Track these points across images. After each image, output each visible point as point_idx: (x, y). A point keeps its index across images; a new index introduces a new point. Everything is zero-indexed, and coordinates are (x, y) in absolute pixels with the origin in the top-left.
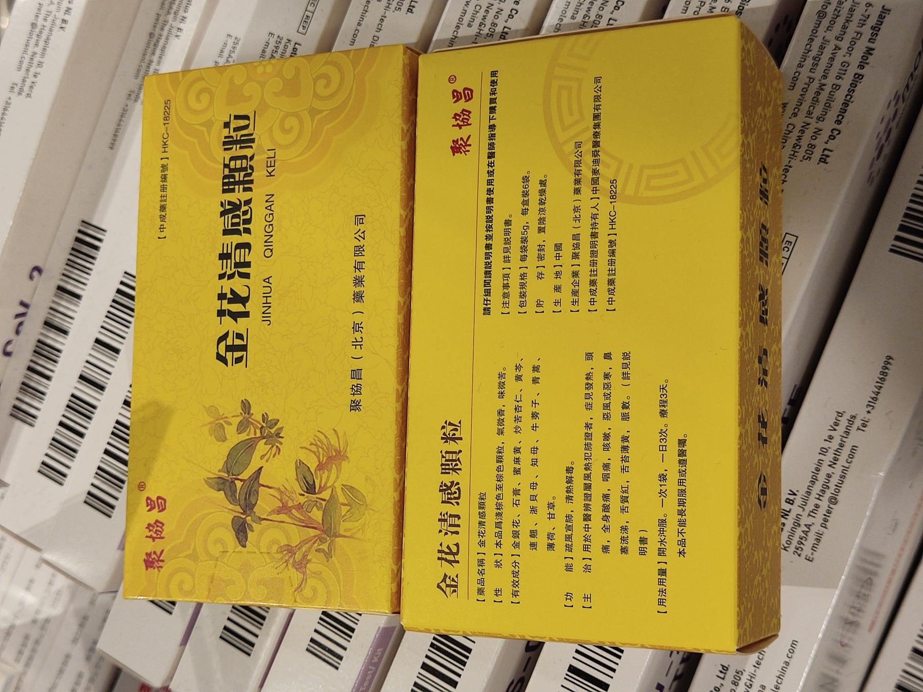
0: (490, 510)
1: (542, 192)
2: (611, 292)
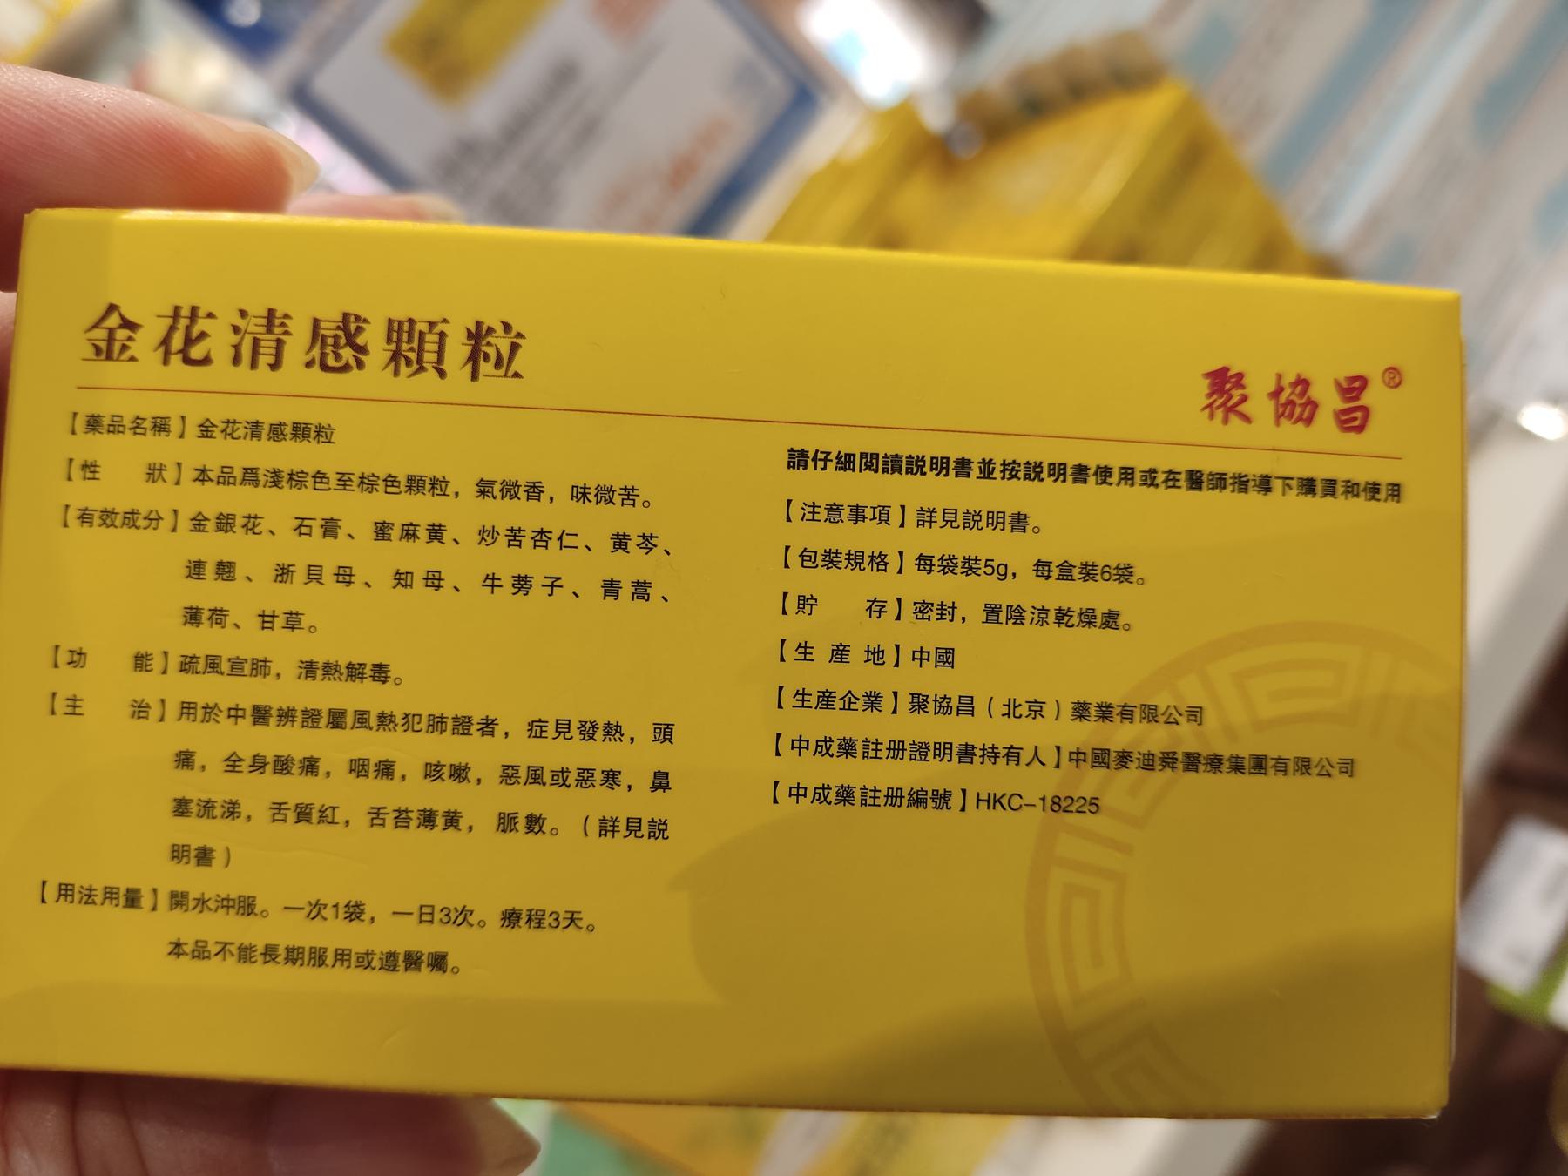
0: (290, 456)
1: (1088, 618)
2: (821, 794)
